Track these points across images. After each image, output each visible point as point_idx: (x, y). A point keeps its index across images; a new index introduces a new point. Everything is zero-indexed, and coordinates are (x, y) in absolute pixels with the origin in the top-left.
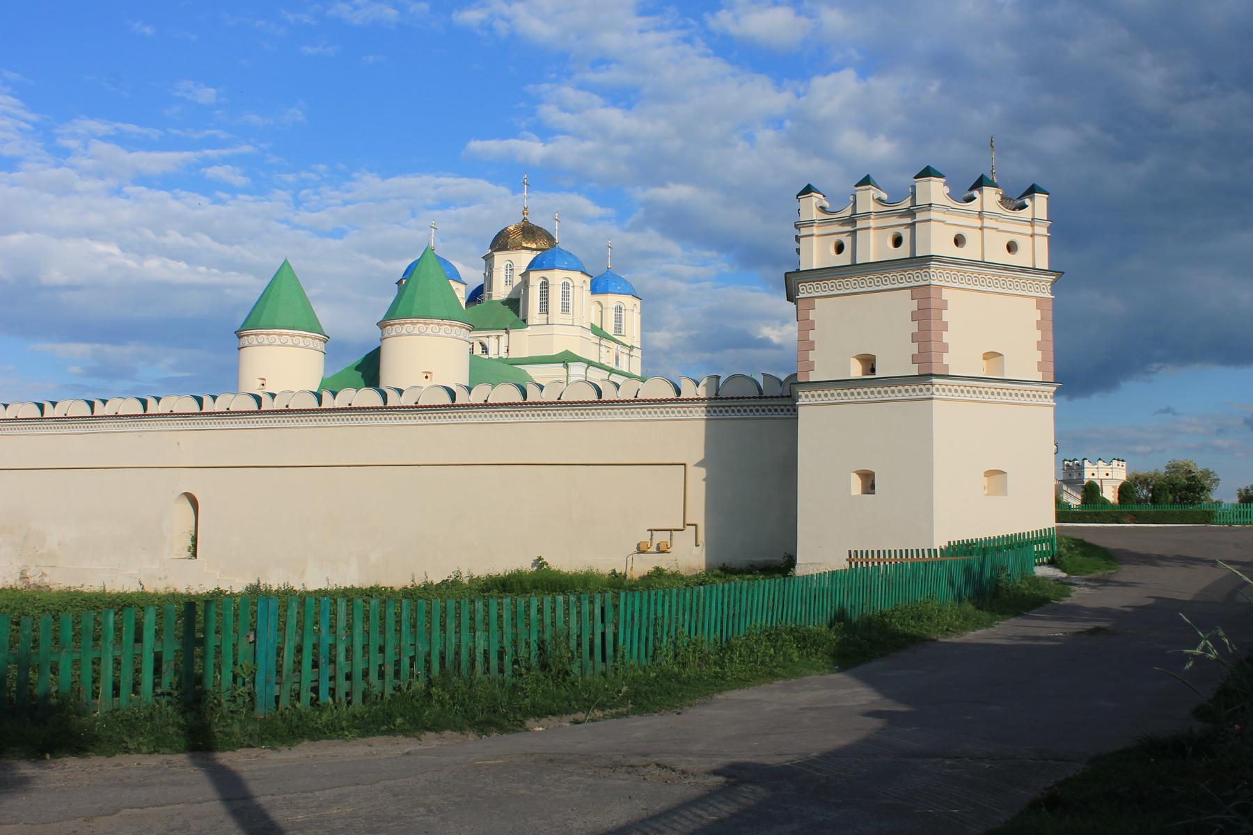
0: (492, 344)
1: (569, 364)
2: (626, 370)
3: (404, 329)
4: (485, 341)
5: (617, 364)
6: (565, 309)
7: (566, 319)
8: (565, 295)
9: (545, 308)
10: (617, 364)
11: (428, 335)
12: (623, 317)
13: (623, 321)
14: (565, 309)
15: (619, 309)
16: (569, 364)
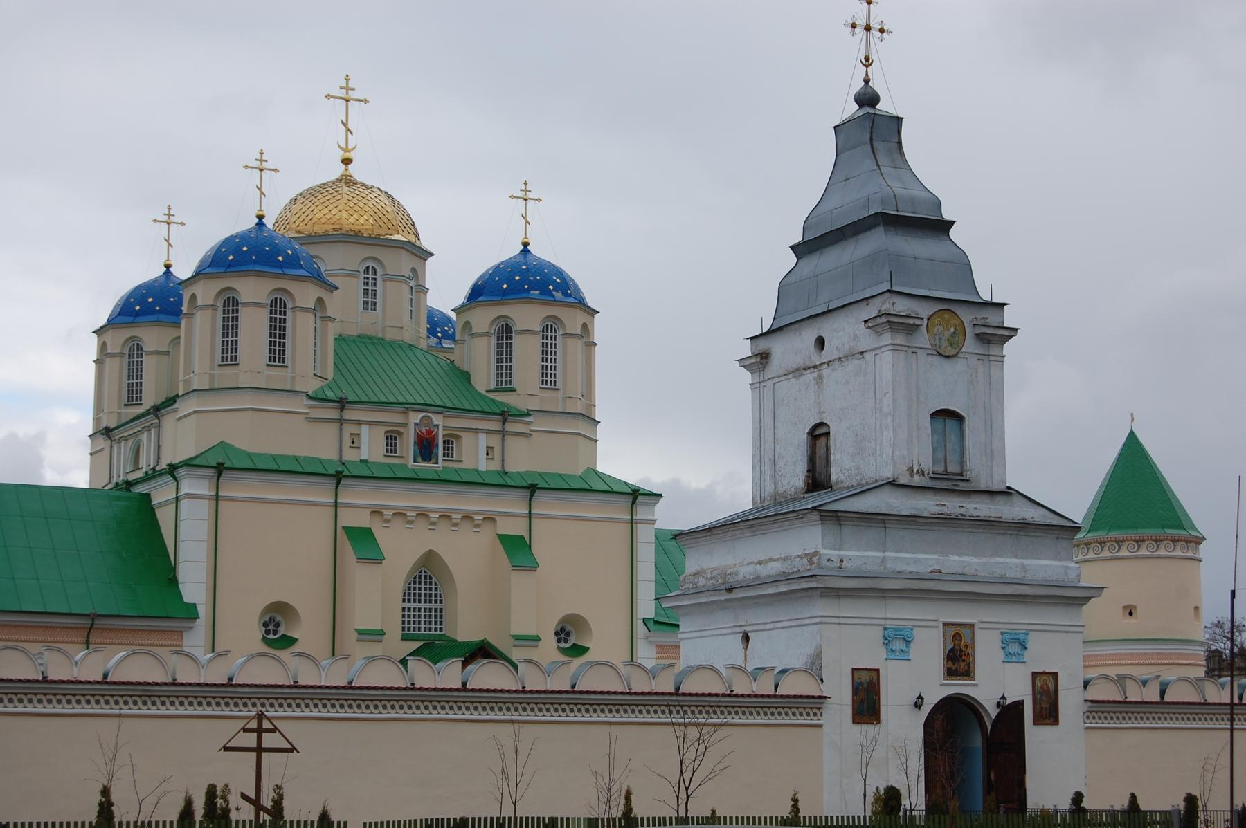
6: (229, 354)
14: (229, 354)
15: (506, 331)
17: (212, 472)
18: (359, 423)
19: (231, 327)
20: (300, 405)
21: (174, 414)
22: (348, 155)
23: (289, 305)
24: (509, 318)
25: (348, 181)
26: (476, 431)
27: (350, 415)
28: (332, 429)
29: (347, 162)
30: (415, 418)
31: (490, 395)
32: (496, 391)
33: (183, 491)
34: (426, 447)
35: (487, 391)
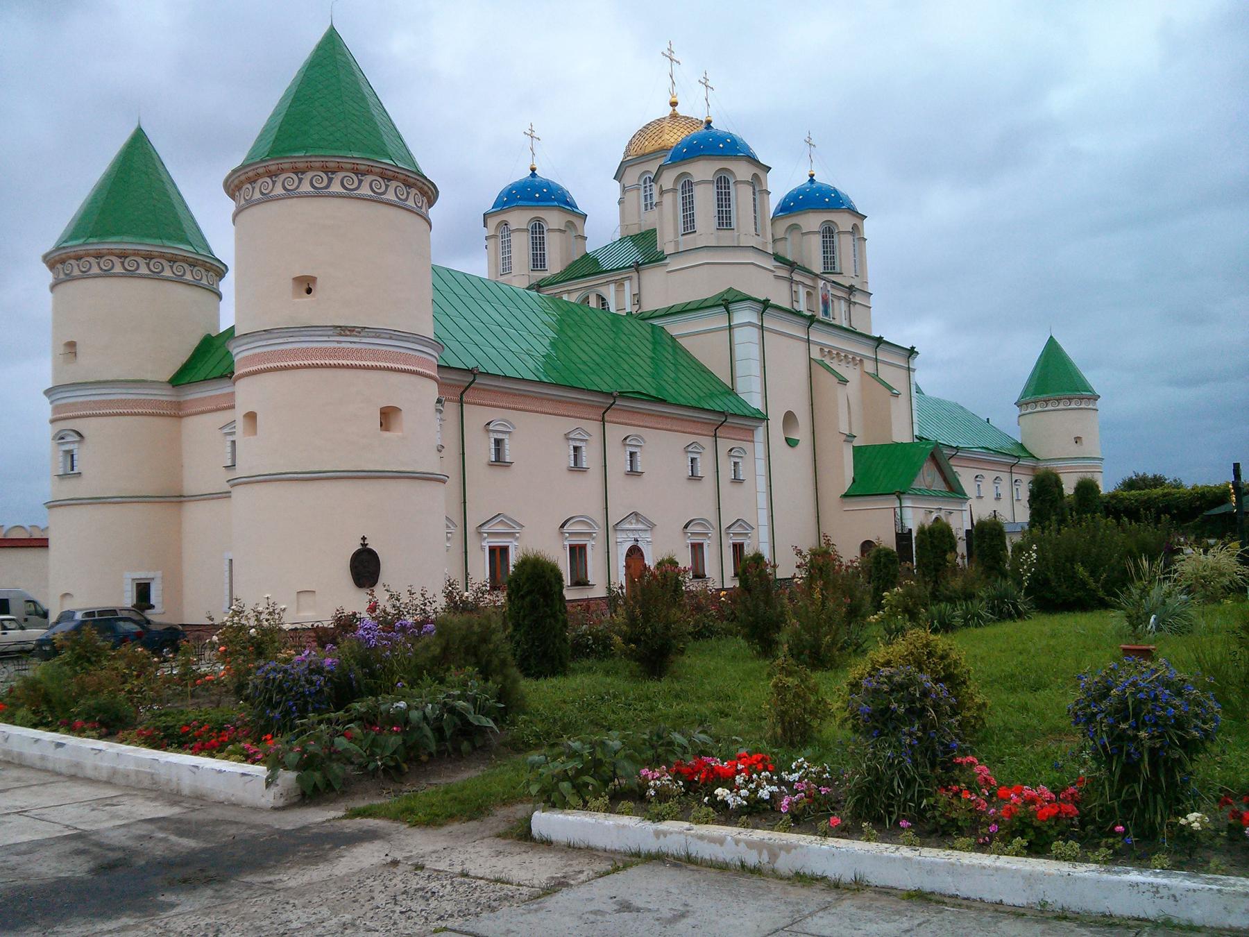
0: (610, 293)
1: (732, 307)
2: (845, 325)
3: (257, 190)
4: (603, 291)
5: (826, 312)
6: (724, 220)
7: (726, 238)
8: (724, 200)
9: (689, 225)
10: (826, 312)
11: (301, 196)
12: (836, 244)
13: (837, 252)
14: (724, 220)
15: (828, 232)
16: (732, 307)
17: (759, 307)
18: (798, 283)
19: (724, 200)
20: (770, 264)
21: (664, 268)
22: (674, 100)
23: (757, 189)
24: (833, 222)
25: (674, 116)
26: (839, 298)
27: (796, 277)
28: (785, 286)
29: (674, 104)
30: (821, 283)
31: (825, 275)
32: (823, 273)
33: (735, 321)
34: (825, 303)
35: (823, 273)
